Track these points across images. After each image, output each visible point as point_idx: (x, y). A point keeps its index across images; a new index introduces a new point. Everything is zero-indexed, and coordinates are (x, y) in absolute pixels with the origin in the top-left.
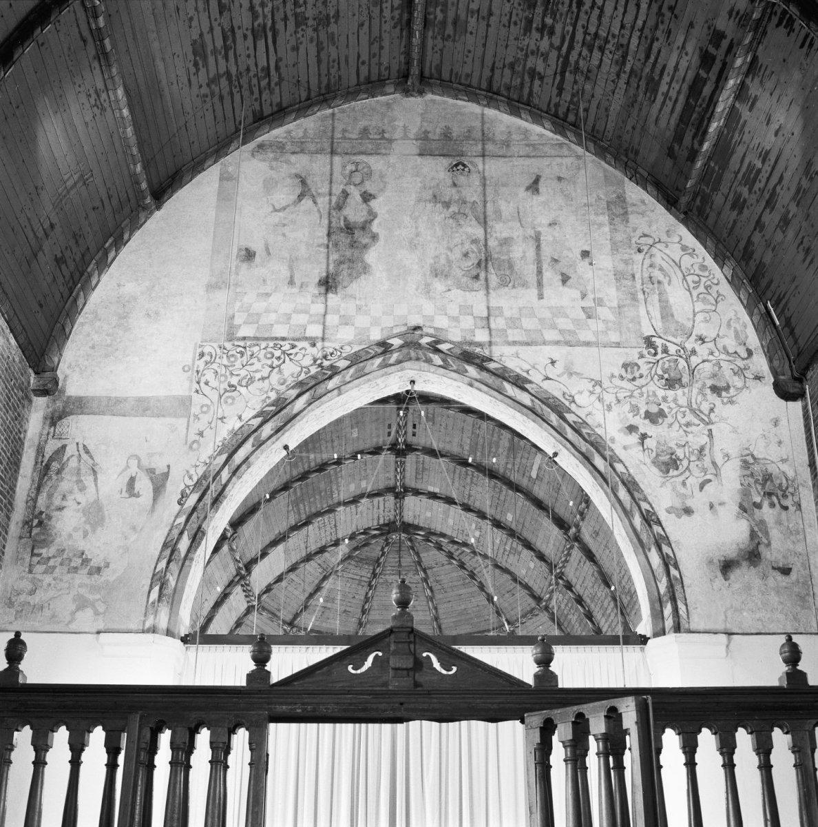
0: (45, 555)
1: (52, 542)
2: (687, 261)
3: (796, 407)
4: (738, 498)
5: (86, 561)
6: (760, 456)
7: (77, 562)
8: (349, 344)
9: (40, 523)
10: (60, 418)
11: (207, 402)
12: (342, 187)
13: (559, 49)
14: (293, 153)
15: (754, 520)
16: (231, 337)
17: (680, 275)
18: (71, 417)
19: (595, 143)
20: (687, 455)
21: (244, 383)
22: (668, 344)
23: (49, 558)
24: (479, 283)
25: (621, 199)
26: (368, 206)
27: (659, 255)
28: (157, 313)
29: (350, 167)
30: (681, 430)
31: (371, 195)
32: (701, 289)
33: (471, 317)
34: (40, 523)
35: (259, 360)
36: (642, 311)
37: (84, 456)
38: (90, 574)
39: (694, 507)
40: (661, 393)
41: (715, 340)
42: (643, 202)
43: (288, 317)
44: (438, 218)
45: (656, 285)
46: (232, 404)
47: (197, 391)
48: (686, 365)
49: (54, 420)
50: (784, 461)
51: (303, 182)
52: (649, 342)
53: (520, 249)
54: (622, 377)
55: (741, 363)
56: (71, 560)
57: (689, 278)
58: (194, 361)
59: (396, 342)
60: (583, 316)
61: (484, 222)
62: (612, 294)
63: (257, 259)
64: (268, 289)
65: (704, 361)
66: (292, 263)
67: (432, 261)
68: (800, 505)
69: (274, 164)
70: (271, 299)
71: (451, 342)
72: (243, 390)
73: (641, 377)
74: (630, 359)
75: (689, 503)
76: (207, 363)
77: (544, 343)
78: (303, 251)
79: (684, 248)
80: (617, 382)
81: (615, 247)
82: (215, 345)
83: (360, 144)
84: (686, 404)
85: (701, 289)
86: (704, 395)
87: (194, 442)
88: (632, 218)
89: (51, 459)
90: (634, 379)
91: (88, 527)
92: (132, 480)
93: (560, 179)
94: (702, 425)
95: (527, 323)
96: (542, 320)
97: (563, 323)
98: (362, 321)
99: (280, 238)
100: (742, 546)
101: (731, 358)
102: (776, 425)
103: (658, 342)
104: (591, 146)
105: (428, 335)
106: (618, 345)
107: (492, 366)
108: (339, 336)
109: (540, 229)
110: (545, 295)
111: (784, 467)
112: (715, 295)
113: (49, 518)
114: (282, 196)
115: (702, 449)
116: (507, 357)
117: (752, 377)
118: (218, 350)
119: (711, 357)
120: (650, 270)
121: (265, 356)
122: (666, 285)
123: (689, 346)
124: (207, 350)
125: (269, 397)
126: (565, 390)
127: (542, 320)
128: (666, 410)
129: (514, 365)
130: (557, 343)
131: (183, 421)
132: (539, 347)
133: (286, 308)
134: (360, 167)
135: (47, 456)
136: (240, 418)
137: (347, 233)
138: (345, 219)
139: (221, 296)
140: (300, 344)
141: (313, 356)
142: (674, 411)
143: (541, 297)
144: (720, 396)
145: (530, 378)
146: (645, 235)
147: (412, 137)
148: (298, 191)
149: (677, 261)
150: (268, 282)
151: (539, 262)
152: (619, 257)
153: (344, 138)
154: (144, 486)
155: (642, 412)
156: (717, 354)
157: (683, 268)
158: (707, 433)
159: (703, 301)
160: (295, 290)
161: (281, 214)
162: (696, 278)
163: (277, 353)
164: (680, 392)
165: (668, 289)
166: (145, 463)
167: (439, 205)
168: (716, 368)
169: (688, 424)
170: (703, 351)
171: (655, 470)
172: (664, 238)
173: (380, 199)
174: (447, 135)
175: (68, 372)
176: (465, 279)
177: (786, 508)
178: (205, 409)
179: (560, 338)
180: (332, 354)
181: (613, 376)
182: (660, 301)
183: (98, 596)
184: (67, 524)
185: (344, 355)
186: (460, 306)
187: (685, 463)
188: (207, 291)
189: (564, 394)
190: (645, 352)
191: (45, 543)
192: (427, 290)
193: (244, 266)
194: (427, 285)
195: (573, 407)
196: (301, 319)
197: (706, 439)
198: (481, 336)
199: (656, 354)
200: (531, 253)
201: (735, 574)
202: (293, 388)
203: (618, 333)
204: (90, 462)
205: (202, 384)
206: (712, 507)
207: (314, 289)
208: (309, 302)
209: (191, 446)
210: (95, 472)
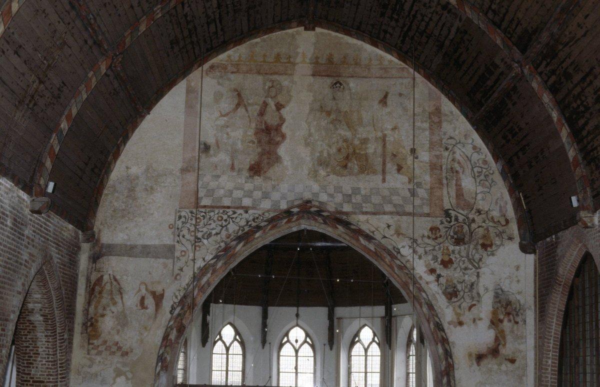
0: (96, 344)
1: (100, 336)
2: (475, 157)
3: (531, 258)
4: (490, 316)
5: (119, 348)
6: (506, 290)
7: (114, 349)
8: (268, 211)
9: (92, 325)
10: (98, 258)
11: (184, 249)
12: (263, 99)
13: (402, 28)
14: (232, 73)
15: (498, 330)
16: (197, 206)
17: (470, 167)
18: (105, 257)
19: (424, 70)
20: (463, 288)
21: (206, 237)
22: (459, 215)
23: (98, 346)
24: (347, 171)
25: (438, 111)
26: (280, 113)
27: (458, 152)
28: (152, 188)
29: (269, 84)
30: (461, 273)
31: (281, 105)
32: (482, 177)
33: (341, 194)
34: (92, 325)
35: (214, 222)
36: (445, 192)
37: (115, 283)
38: (122, 355)
39: (465, 322)
40: (451, 248)
41: (487, 212)
42: (452, 113)
43: (231, 192)
44: (323, 123)
45: (455, 174)
46: (199, 250)
47: (178, 242)
48: (468, 229)
49: (95, 258)
50: (520, 293)
51: (239, 95)
52: (447, 213)
53: (373, 147)
54: (429, 237)
55: (501, 229)
56: (111, 348)
57: (476, 170)
58: (175, 221)
59: (295, 210)
60: (408, 194)
61: (350, 126)
62: (427, 179)
63: (212, 152)
64: (219, 173)
65: (479, 227)
66: (233, 154)
67: (318, 154)
68: (525, 321)
69: (220, 81)
70: (220, 180)
71: (329, 212)
72: (205, 241)
73: (441, 236)
74: (435, 225)
75: (462, 319)
76: (183, 223)
77: (384, 213)
78: (239, 146)
79: (475, 148)
80: (427, 240)
81: (432, 146)
82: (188, 211)
83: (275, 66)
84: (465, 255)
85: (482, 177)
86: (477, 250)
87: (178, 274)
88: (444, 125)
89: (95, 284)
90: (436, 238)
91: (119, 327)
92: (143, 299)
93: (400, 95)
94: (474, 269)
95: (376, 200)
96: (384, 198)
97: (396, 199)
98: (276, 196)
99: (225, 136)
100: (490, 346)
101: (495, 225)
102: (517, 270)
103: (453, 213)
104: (422, 71)
105: (314, 206)
106: (428, 215)
107: (353, 227)
108: (261, 206)
109: (386, 132)
110: (386, 180)
111: (518, 297)
112: (490, 181)
113: (97, 321)
114: (226, 105)
115: (472, 285)
116: (363, 222)
117: (507, 238)
118: (190, 214)
119: (483, 224)
120: (452, 163)
121: (218, 219)
122: (461, 173)
123: (471, 216)
124: (183, 214)
125: (220, 246)
126: (395, 245)
127: (384, 198)
128: (454, 259)
129: (364, 228)
130: (391, 213)
131: (171, 261)
132: (381, 216)
133: (230, 185)
134: (275, 84)
135: (93, 282)
136: (204, 259)
137: (267, 133)
138: (265, 122)
139: (191, 177)
140: (239, 211)
141: (246, 219)
142: (458, 260)
143: (384, 180)
144: (486, 250)
145: (374, 237)
146: (451, 138)
147: (308, 61)
148: (236, 101)
149: (469, 156)
150: (219, 168)
151: (384, 155)
152: (434, 153)
153: (264, 61)
154: (150, 302)
155: (439, 260)
156: (487, 222)
157: (472, 162)
158: (476, 274)
159: (482, 186)
160: (235, 174)
161: (225, 118)
162: (480, 170)
163: (225, 217)
164: (462, 248)
165: (462, 176)
166: (150, 288)
167: (324, 114)
168: (486, 232)
169: (466, 269)
170: (479, 219)
171: (443, 297)
172: (463, 140)
173: (287, 108)
174: (330, 60)
175: (102, 227)
176: (338, 168)
177: (517, 323)
178: (183, 253)
179: (394, 210)
180: (258, 218)
181: (423, 236)
182: (456, 185)
183: (128, 369)
184: (107, 324)
185: (265, 219)
186: (335, 187)
187: (462, 293)
188: (181, 173)
189: (394, 247)
190: (444, 221)
191: (97, 336)
192: (314, 174)
193: (203, 156)
194: (316, 171)
195: (399, 256)
196: (238, 194)
197: (475, 278)
198: (347, 208)
199: (450, 222)
200: (380, 150)
201: (485, 362)
202: (234, 240)
203: (429, 207)
204: (118, 286)
205: (181, 237)
206: (474, 321)
207: (246, 173)
208: (244, 182)
209: (176, 277)
210: (121, 294)
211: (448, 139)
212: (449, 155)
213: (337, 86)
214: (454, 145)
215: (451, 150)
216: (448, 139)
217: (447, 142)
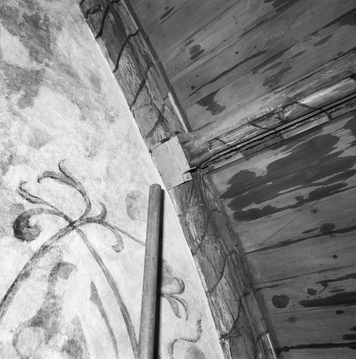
42: (96, 81)
88: (46, 97)
146: (67, 179)
211: (50, 175)
212: (24, 275)
214: (72, 224)
215: (45, 248)
216: (50, 175)
217: (32, 188)
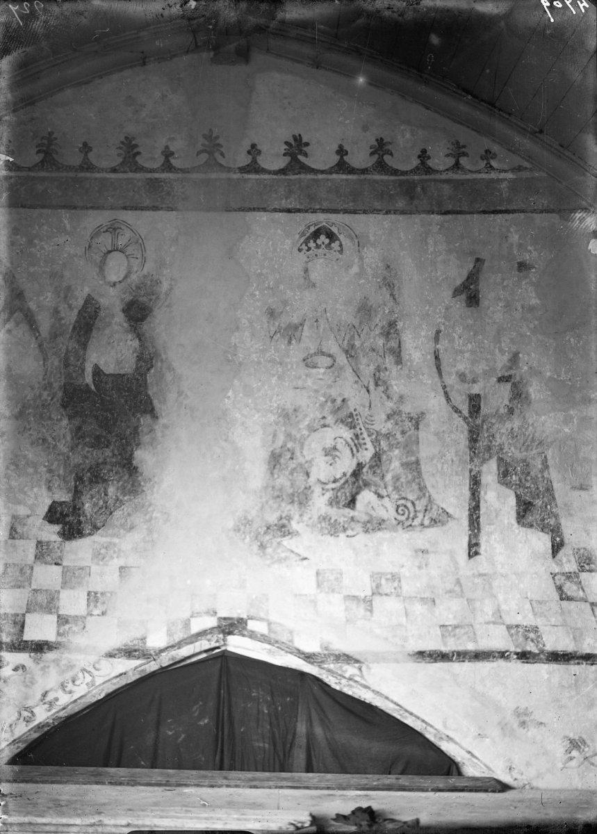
143: (473, 550)
213: (319, 242)
